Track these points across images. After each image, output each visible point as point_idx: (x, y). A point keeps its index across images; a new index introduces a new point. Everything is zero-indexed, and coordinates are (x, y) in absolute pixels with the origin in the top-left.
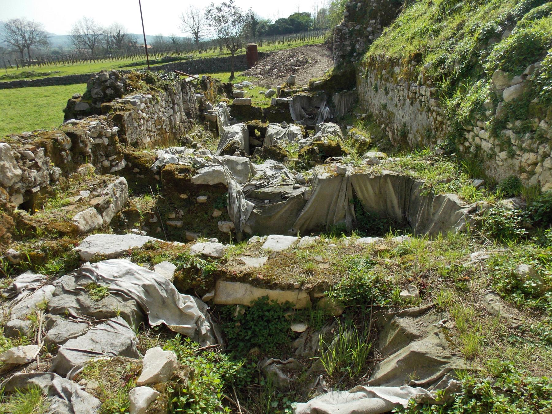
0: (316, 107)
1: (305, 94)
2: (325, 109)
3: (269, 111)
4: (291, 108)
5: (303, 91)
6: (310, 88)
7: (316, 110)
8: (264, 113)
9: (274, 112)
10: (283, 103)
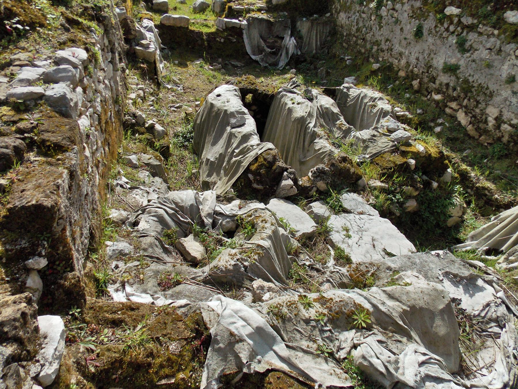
0: (277, 37)
1: (263, 16)
2: (290, 40)
3: (215, 38)
4: (245, 36)
5: (260, 10)
6: (268, 7)
7: (279, 41)
8: (207, 41)
9: (222, 40)
10: (233, 27)
